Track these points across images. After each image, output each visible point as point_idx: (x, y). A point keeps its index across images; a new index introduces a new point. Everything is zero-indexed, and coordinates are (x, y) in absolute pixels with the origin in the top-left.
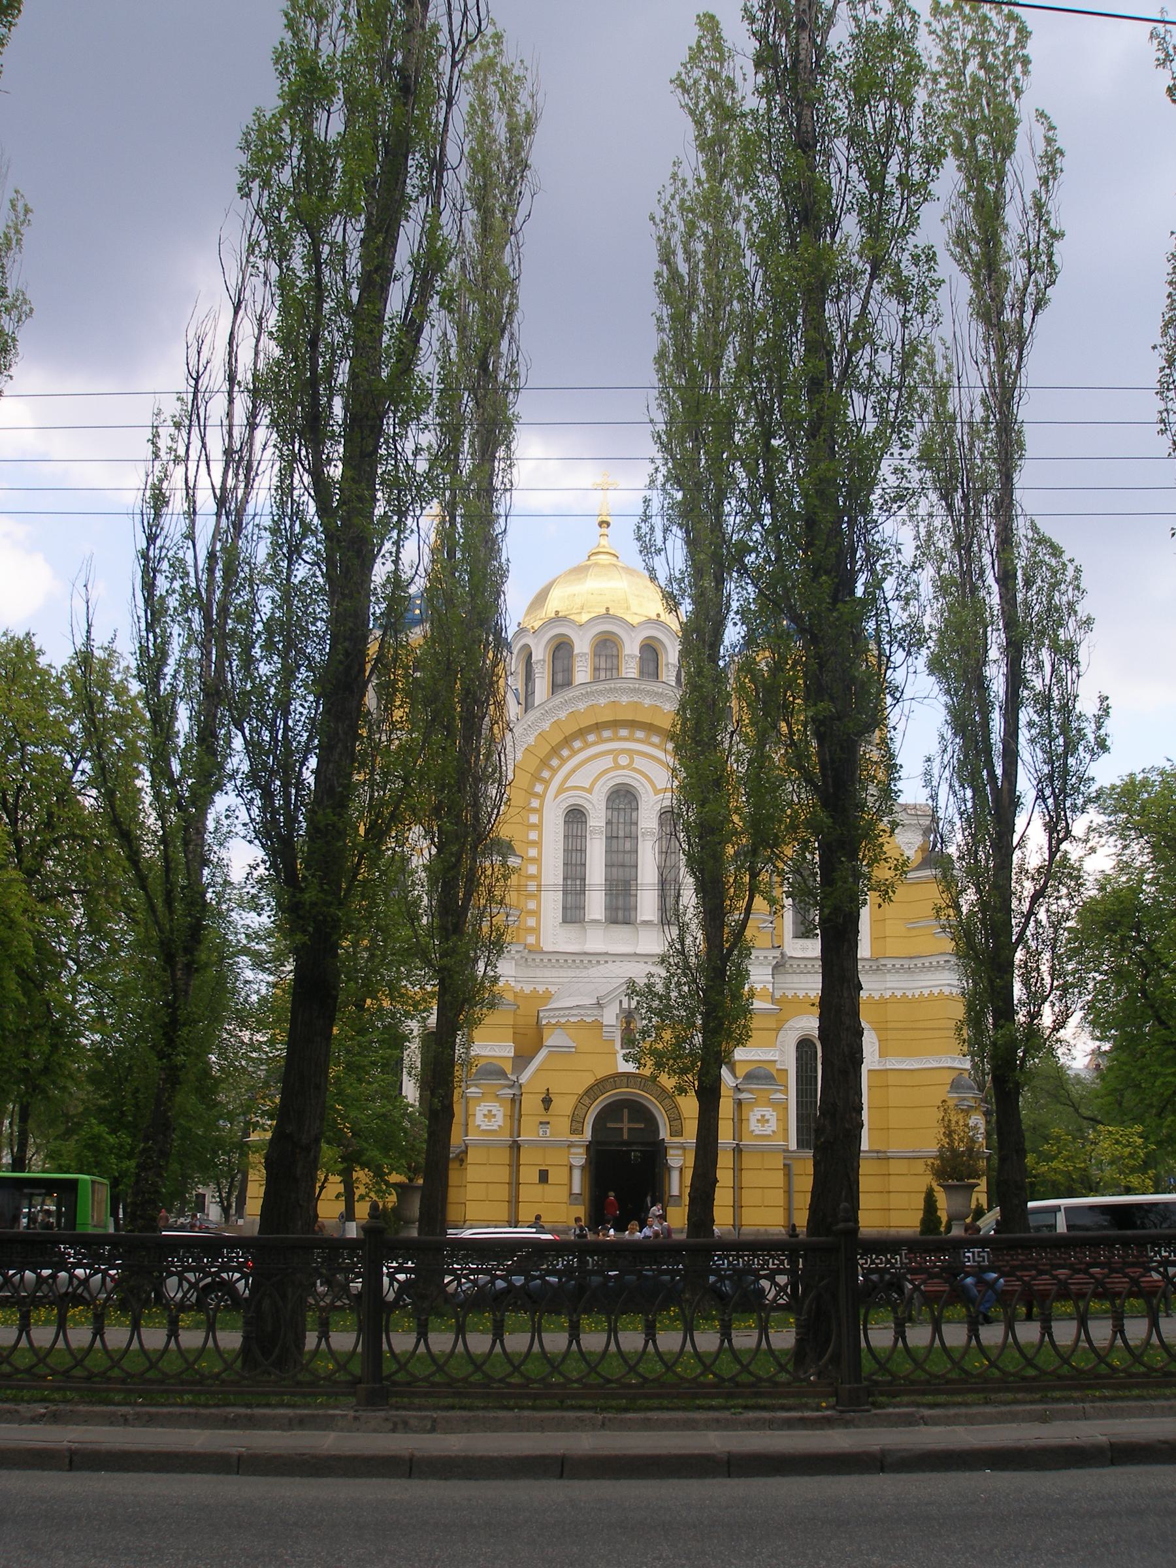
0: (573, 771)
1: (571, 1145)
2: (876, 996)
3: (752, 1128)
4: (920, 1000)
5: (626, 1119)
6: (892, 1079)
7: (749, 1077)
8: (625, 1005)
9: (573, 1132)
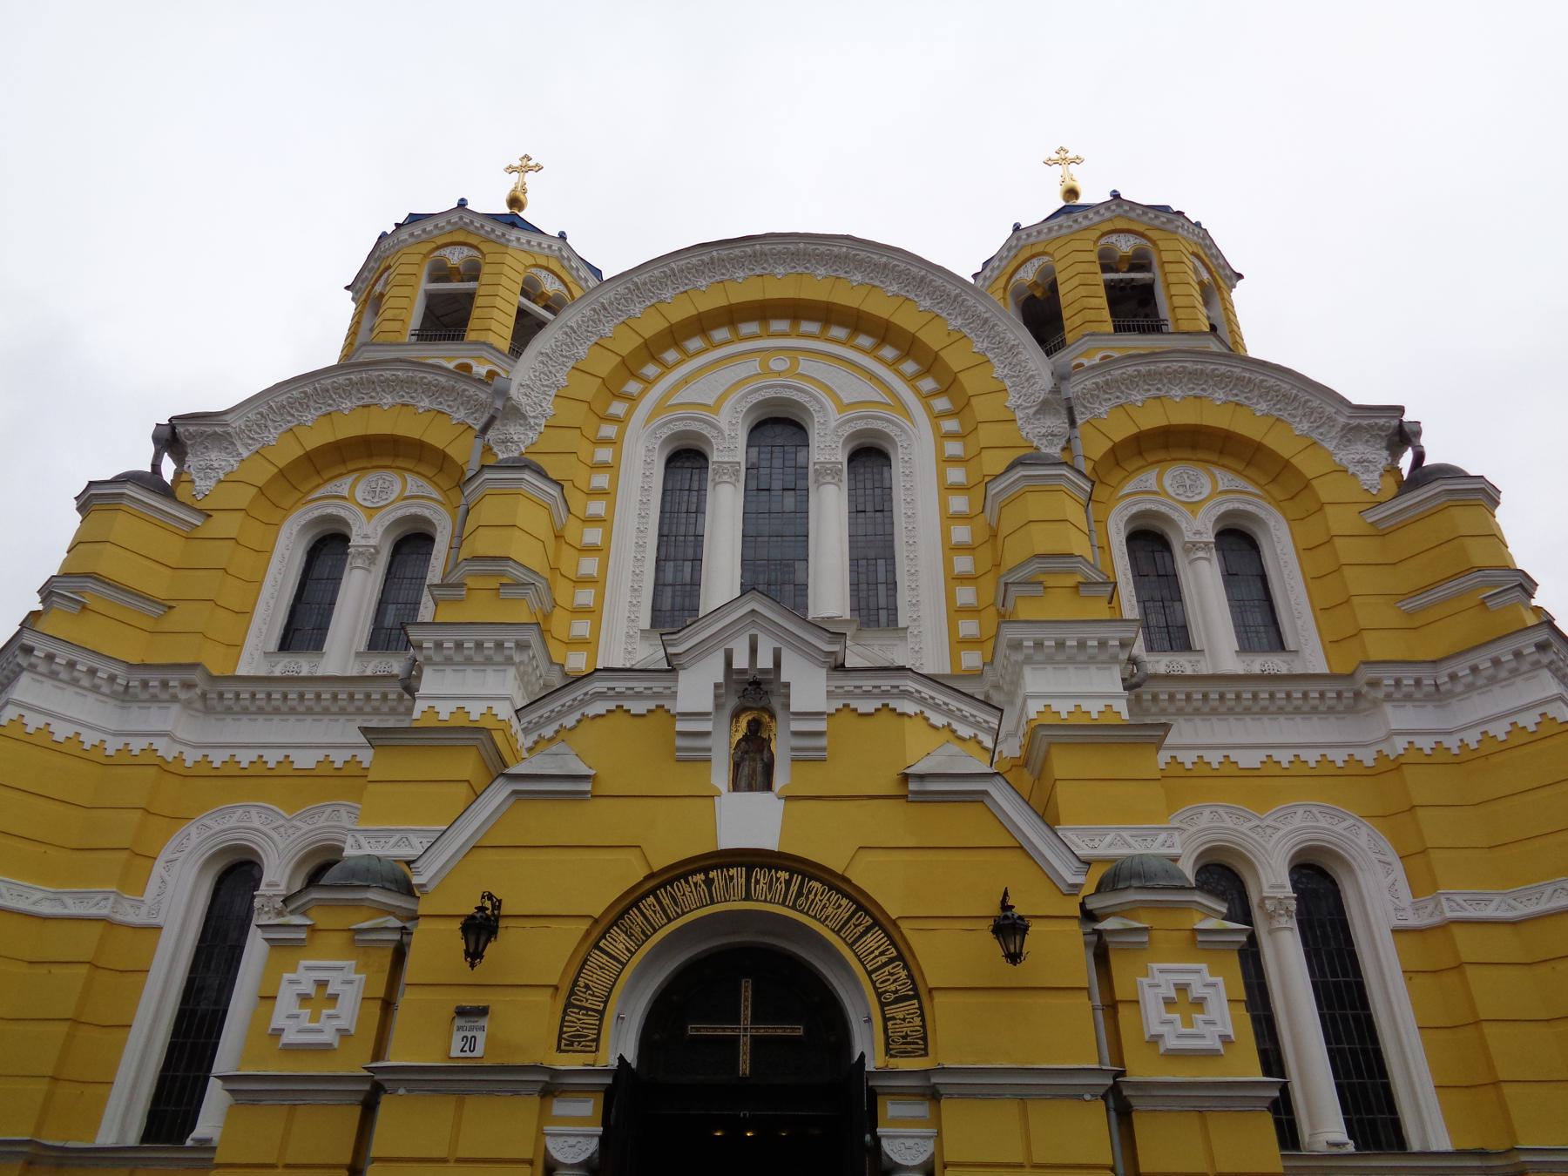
0: (685, 381)
1: (552, 1086)
2: (1367, 757)
3: (1155, 1028)
4: (1486, 754)
5: (746, 1011)
6: (1468, 945)
7: (1109, 884)
8: (741, 661)
9: (566, 1043)
